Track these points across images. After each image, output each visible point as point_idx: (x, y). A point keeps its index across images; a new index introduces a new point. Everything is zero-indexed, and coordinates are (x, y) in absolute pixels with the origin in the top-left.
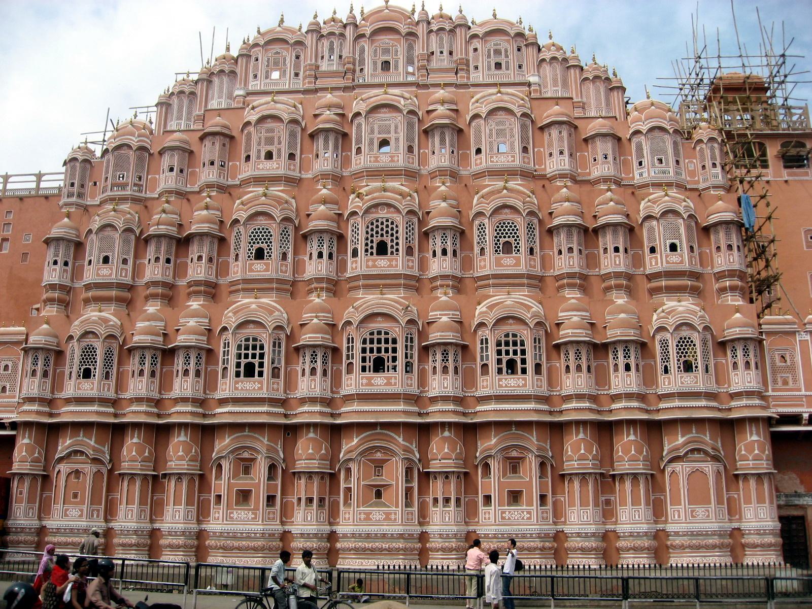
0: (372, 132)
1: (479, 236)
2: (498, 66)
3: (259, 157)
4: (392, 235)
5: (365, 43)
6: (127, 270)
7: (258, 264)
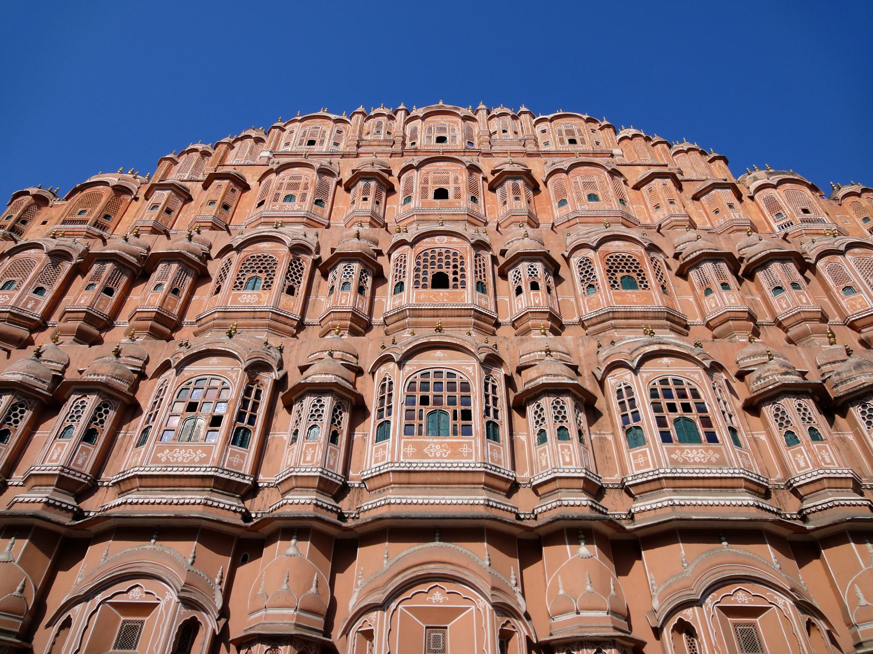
0: (426, 181)
1: (581, 273)
2: (572, 142)
3: (276, 200)
4: (455, 266)
5: (418, 123)
6: (37, 302)
7: (247, 294)
